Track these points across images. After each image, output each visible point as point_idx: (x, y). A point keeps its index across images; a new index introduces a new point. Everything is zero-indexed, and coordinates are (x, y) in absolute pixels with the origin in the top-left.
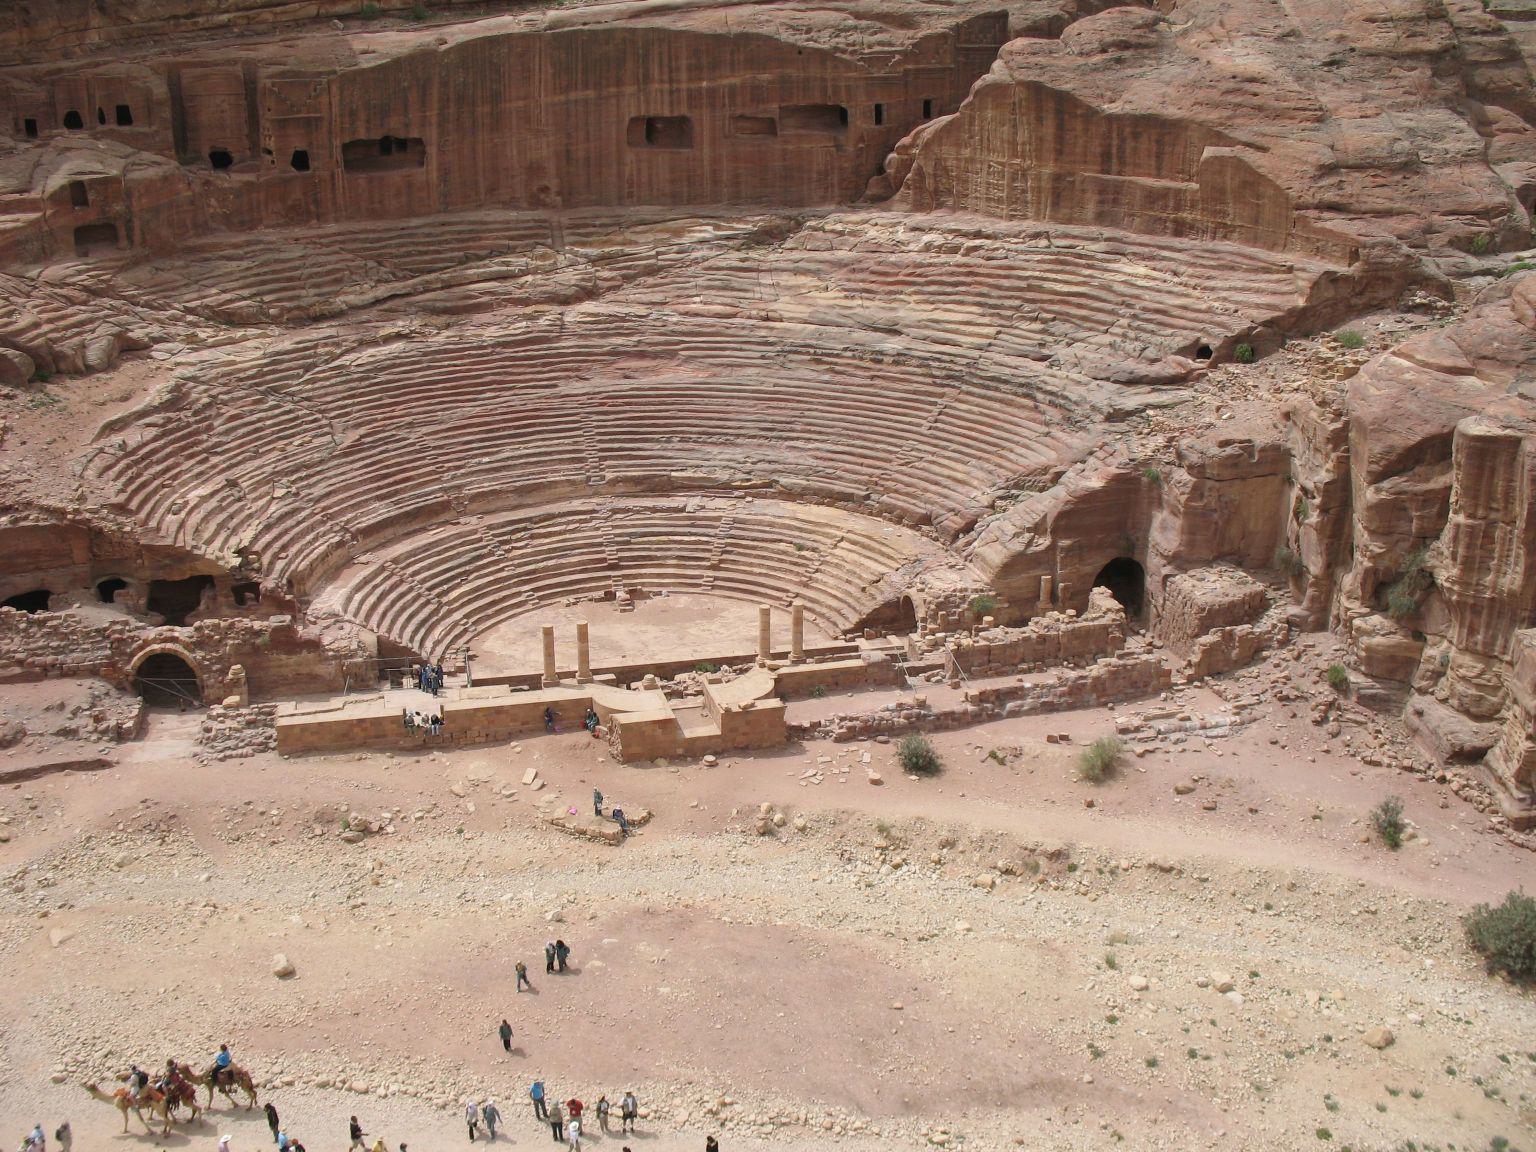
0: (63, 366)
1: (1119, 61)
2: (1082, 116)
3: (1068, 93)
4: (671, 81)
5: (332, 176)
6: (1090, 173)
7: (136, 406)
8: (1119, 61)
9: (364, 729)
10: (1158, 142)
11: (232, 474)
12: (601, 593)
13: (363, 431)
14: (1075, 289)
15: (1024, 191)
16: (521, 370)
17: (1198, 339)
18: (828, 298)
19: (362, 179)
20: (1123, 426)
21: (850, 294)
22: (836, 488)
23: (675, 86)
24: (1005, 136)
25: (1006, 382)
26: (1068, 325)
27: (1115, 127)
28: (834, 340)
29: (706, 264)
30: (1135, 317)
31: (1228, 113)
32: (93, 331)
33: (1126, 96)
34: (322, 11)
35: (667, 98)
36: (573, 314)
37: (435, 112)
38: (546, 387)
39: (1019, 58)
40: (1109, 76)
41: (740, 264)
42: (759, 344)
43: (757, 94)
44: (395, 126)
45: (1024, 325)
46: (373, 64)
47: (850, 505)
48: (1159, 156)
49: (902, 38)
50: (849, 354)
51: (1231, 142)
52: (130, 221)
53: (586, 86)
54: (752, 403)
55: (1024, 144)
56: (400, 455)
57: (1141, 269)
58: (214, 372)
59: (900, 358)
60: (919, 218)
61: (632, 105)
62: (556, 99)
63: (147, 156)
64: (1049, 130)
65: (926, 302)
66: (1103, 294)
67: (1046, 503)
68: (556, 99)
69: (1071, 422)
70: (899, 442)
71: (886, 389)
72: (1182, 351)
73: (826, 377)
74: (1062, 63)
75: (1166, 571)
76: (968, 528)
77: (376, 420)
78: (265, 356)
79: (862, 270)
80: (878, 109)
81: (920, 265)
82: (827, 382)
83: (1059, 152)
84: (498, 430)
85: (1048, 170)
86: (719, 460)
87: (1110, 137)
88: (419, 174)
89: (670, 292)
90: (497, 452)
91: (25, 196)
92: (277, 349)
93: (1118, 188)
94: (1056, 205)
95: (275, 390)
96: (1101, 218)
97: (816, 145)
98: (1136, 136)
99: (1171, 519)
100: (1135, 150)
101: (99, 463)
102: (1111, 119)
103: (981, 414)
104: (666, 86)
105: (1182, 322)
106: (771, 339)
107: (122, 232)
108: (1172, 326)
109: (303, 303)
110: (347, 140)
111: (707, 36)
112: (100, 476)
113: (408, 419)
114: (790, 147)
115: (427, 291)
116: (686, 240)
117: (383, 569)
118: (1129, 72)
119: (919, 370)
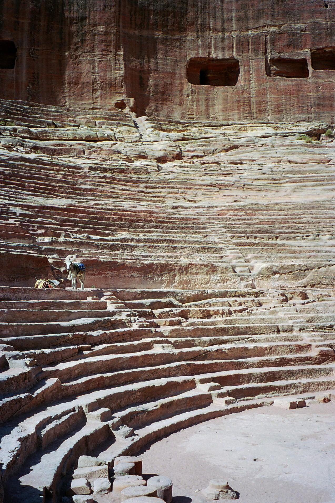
23: (227, 34)
36: (167, 166)
68: (132, 32)
104: (220, 34)
114: (321, 81)
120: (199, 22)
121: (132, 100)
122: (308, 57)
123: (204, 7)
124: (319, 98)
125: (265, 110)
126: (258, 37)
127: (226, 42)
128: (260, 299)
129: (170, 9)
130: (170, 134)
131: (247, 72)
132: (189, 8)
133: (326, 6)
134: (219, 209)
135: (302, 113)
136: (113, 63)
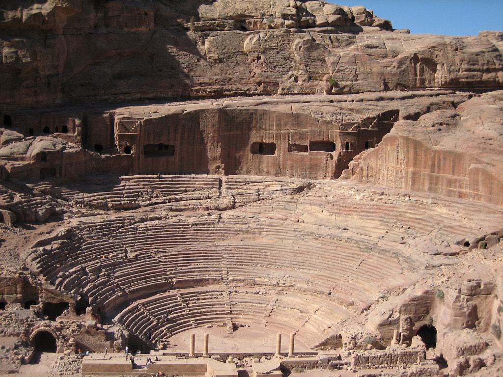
0: (27, 219)
1: (440, 130)
3: (419, 141)
4: (269, 130)
5: (139, 157)
6: (427, 171)
7: (53, 235)
8: (440, 130)
9: (117, 368)
11: (83, 265)
12: (222, 324)
13: (137, 253)
14: (418, 217)
15: (401, 178)
16: (202, 235)
17: (464, 239)
18: (324, 215)
19: (150, 159)
20: (433, 271)
21: (331, 214)
22: (318, 290)
23: (271, 131)
24: (395, 157)
25: (388, 252)
26: (414, 231)
28: (324, 231)
29: (278, 199)
30: (440, 229)
31: (480, 151)
32: (41, 207)
33: (441, 143)
34: (142, 97)
35: (267, 136)
37: (179, 136)
38: (211, 242)
39: (401, 128)
40: (435, 135)
41: (290, 200)
42: (294, 231)
43: (302, 137)
44: (163, 140)
45: (397, 230)
46: (158, 117)
48: (454, 167)
49: (358, 118)
50: (329, 237)
51: (480, 162)
52: (61, 168)
53: (237, 129)
54: (289, 254)
56: (151, 264)
57: (444, 210)
58: (84, 226)
59: (348, 240)
60: (361, 186)
61: (254, 138)
62: (225, 134)
63: (71, 144)
64: (411, 155)
65: (360, 218)
66: (428, 220)
67: (397, 301)
69: (412, 269)
70: (344, 273)
72: (458, 243)
73: (319, 246)
74: (417, 130)
75: (444, 331)
76: (368, 309)
77: (144, 249)
78: (104, 221)
79: (336, 205)
80: (347, 144)
81: (359, 204)
82: (319, 248)
83: (415, 165)
84: (190, 257)
85: (411, 170)
86: (276, 275)
87: (435, 159)
88: (172, 158)
89: (262, 209)
90: (189, 265)
91: (24, 155)
92: (109, 219)
93: (437, 178)
94: (413, 183)
95: (107, 235)
97: (322, 155)
98: (445, 159)
99: (448, 310)
100: (444, 164)
101: (33, 255)
102: (435, 152)
103: (377, 264)
104: (268, 131)
105: (459, 232)
106: (299, 230)
107: (58, 172)
108: (454, 233)
109: (122, 202)
110: (146, 144)
111: (284, 114)
112: (33, 260)
113: (156, 250)
115: (169, 202)
116: (270, 189)
117: (137, 307)
118: (444, 134)
119: (354, 245)
120: (258, 126)
121: (223, 165)
122: (308, 145)
123: (261, 119)
124: (311, 165)
125: (286, 168)
126: (286, 134)
127: (270, 135)
128: (223, 293)
129: (244, 121)
130: (233, 191)
131: (279, 150)
132: (254, 120)
133: (319, 122)
134: (232, 247)
135: (303, 171)
136: (216, 149)
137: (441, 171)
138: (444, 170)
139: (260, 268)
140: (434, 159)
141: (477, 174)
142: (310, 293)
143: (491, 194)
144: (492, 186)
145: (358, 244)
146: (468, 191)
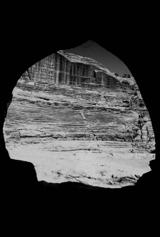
2: (66, 61)
3: (63, 56)
6: (68, 74)
10: (83, 69)
24: (47, 63)
27: (73, 65)
47: (84, 138)
48: (83, 72)
55: (52, 65)
64: (58, 63)
71: (61, 111)
85: (58, 72)
87: (72, 67)
93: (75, 78)
94: (60, 80)
96: (71, 83)
102: (72, 63)
119: (66, 107)
137: (76, 74)
138: (77, 73)
139: (11, 122)
140: (71, 67)
141: (101, 75)
142: (70, 138)
143: (108, 85)
144: (109, 81)
145: (68, 106)
146: (95, 84)
